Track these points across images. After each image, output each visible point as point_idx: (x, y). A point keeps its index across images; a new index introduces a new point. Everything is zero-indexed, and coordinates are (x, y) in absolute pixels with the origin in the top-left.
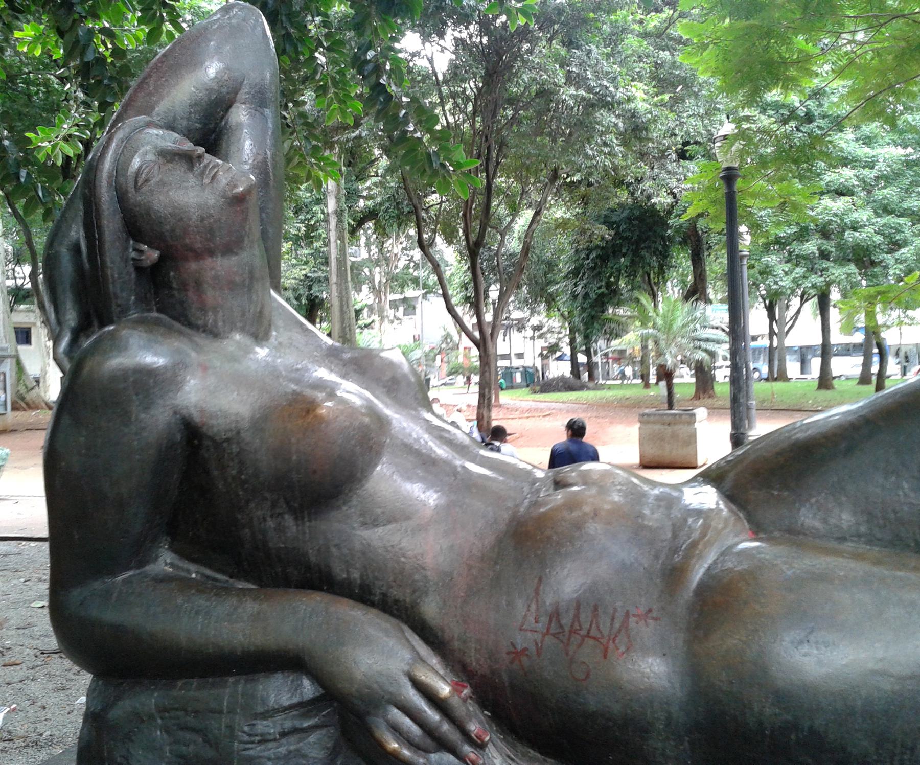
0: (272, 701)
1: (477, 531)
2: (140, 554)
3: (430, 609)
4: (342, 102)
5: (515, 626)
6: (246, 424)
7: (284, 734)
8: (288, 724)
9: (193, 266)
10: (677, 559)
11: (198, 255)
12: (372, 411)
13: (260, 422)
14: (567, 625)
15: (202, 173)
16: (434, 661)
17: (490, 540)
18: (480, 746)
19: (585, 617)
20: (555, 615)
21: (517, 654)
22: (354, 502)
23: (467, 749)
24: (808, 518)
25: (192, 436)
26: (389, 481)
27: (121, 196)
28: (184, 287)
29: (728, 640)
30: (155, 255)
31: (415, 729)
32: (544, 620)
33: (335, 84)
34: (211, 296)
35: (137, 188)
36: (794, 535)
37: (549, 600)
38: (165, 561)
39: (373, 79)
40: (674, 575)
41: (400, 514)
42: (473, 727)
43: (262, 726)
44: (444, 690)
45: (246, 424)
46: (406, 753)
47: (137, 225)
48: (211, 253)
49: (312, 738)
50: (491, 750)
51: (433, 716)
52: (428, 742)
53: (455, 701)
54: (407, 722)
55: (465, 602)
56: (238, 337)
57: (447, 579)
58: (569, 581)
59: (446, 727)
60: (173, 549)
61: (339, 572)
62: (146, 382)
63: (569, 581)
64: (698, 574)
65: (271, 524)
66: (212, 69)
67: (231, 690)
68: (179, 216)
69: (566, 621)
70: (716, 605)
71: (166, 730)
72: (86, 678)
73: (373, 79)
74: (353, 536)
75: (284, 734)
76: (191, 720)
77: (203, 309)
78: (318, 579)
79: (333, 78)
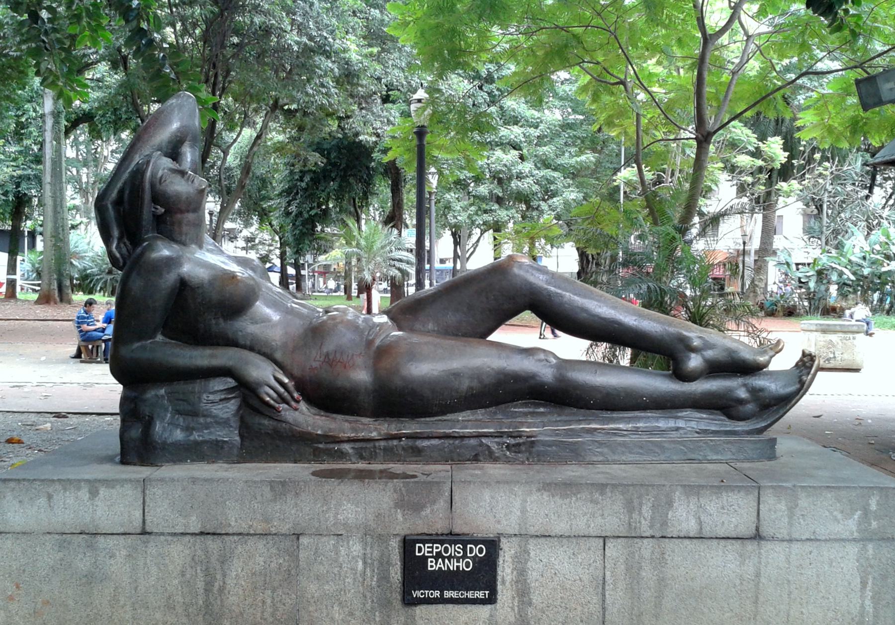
0: (216, 388)
1: (297, 327)
2: (153, 336)
3: (278, 356)
4: (94, 30)
5: (311, 362)
6: (206, 282)
7: (221, 400)
8: (223, 397)
9: (179, 216)
10: (371, 338)
11: (182, 212)
12: (253, 279)
13: (211, 282)
14: (330, 361)
15: (188, 179)
17: (301, 331)
19: (338, 355)
20: (327, 355)
21: (312, 369)
22: (248, 314)
23: (293, 403)
24: (418, 326)
25: (183, 285)
26: (262, 308)
27: (153, 186)
28: (173, 224)
29: (386, 363)
30: (163, 210)
31: (275, 395)
32: (323, 357)
33: (90, 15)
34: (185, 229)
35: (160, 183)
36: (412, 330)
37: (325, 351)
38: (160, 338)
39: (134, 23)
40: (370, 343)
41: (266, 320)
42: (296, 395)
43: (211, 397)
44: (286, 380)
45: (206, 282)
46: (272, 402)
47: (158, 197)
48: (188, 211)
49: (233, 401)
51: (282, 390)
52: (279, 400)
54: (271, 392)
55: (293, 352)
56: (194, 246)
57: (285, 345)
58: (330, 346)
59: (286, 394)
60: (163, 334)
61: (242, 342)
62: (171, 263)
63: (330, 346)
64: (377, 342)
65: (214, 322)
66: (175, 125)
67: (197, 386)
68: (178, 195)
69: (331, 357)
70: (381, 353)
72: (120, 387)
73: (134, 23)
74: (246, 327)
76: (181, 397)
77: (181, 234)
78: (232, 342)
79: (87, 10)
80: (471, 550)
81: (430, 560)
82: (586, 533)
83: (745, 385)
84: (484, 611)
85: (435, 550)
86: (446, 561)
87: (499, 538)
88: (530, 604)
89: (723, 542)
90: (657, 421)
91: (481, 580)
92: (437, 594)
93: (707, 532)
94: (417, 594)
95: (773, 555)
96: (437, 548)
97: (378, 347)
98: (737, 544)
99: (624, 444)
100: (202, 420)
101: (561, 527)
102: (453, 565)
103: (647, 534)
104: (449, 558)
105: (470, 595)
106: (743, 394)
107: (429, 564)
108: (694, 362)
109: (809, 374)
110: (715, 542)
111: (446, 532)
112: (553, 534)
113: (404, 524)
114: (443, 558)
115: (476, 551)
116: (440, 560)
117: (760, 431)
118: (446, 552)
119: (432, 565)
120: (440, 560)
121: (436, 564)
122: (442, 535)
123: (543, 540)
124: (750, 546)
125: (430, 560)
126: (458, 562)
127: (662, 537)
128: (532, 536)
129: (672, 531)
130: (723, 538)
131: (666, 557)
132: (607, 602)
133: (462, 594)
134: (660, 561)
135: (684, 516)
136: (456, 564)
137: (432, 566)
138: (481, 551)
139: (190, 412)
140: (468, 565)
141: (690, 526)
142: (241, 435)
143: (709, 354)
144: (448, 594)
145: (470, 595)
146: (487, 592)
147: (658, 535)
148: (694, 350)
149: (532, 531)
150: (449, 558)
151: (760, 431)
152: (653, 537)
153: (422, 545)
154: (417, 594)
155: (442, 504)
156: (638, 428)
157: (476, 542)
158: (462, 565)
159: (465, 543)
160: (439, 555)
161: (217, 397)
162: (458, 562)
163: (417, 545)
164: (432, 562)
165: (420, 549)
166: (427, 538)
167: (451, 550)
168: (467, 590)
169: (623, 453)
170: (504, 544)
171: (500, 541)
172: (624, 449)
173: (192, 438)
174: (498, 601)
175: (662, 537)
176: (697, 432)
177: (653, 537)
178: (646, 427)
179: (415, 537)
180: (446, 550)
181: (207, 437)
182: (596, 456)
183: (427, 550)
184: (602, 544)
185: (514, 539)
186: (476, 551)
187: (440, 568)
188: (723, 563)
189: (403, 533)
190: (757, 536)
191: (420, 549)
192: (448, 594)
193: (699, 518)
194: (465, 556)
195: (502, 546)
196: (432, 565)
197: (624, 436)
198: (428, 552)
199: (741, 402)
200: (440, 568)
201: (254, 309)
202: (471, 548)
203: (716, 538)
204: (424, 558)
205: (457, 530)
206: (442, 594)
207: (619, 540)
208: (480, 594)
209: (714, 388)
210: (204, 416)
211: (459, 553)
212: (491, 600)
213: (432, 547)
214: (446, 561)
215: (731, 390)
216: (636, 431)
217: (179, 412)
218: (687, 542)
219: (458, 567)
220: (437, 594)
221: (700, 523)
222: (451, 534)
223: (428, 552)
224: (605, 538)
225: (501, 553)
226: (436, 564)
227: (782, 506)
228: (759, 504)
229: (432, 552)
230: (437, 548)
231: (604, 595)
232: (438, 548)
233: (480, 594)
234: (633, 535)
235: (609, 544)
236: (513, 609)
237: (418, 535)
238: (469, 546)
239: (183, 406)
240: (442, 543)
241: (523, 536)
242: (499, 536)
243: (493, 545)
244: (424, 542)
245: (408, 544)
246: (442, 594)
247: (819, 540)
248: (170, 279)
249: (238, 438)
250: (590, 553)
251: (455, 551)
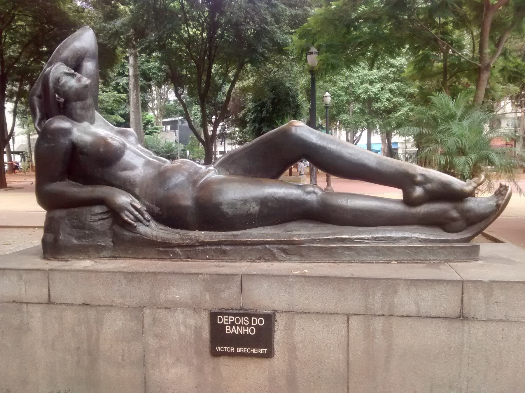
7: (100, 220)
16: (137, 201)
18: (148, 221)
43: (93, 218)
49: (106, 221)
50: (151, 222)
52: (135, 220)
53: (142, 209)
67: (85, 210)
71: (69, 220)
75: (100, 220)
76: (75, 218)
80: (255, 321)
81: (227, 327)
82: (335, 312)
83: (455, 208)
84: (265, 363)
85: (230, 320)
86: (238, 328)
87: (274, 313)
88: (296, 358)
89: (435, 320)
90: (391, 233)
91: (261, 340)
92: (232, 349)
93: (423, 312)
94: (219, 349)
95: (476, 331)
96: (232, 319)
97: (202, 183)
98: (446, 322)
99: (365, 249)
100: (87, 232)
101: (317, 306)
102: (243, 331)
103: (379, 313)
104: (240, 326)
105: (254, 351)
106: (455, 214)
107: (227, 329)
108: (418, 191)
109: (503, 200)
110: (430, 320)
111: (239, 308)
112: (311, 311)
113: (209, 301)
114: (236, 326)
115: (258, 321)
116: (234, 327)
117: (468, 240)
118: (238, 322)
119: (228, 330)
120: (234, 327)
121: (231, 329)
122: (236, 310)
123: (304, 315)
124: (457, 324)
125: (227, 327)
126: (246, 328)
127: (390, 315)
128: (297, 312)
129: (398, 311)
130: (436, 317)
131: (393, 329)
132: (351, 359)
133: (249, 350)
134: (388, 334)
135: (406, 301)
136: (244, 330)
137: (228, 331)
138: (261, 322)
139: (81, 228)
140: (252, 331)
141: (411, 308)
142: (113, 242)
143: (429, 186)
144: (239, 350)
145: (254, 351)
146: (266, 350)
147: (386, 314)
148: (419, 184)
149: (297, 308)
150: (240, 326)
151: (468, 240)
152: (383, 315)
153: (221, 317)
154: (219, 349)
155: (235, 288)
156: (376, 238)
157: (258, 316)
158: (248, 331)
159: (250, 316)
160: (233, 324)
161: (96, 218)
162: (246, 328)
163: (218, 317)
164: (228, 328)
165: (220, 318)
166: (224, 311)
167: (241, 320)
168: (253, 347)
169: (365, 255)
170: (278, 317)
171: (275, 316)
172: (366, 253)
173: (81, 243)
174: (275, 356)
175: (390, 315)
176: (420, 241)
177: (383, 315)
178: (382, 237)
179: (217, 311)
180: (238, 320)
181: (91, 243)
182: (346, 257)
183: (225, 320)
184: (346, 319)
185: (284, 314)
186: (258, 321)
187: (234, 332)
188: (436, 335)
189: (210, 308)
190: (462, 317)
191: (220, 319)
192: (239, 350)
193: (418, 303)
194: (250, 325)
195: (277, 318)
196: (228, 330)
197: (366, 243)
198: (226, 321)
199: (454, 220)
200: (234, 332)
201: (122, 161)
202: (254, 320)
203: (430, 317)
204: (223, 326)
205: (246, 307)
206: (235, 350)
207: (360, 318)
208: (260, 351)
209: (434, 210)
210: (89, 229)
211: (246, 323)
212: (269, 355)
213: (228, 318)
214: (238, 328)
215: (445, 212)
216: (375, 239)
217: (74, 227)
218: (408, 320)
219: (246, 332)
220: (232, 349)
221: (418, 307)
222: (242, 309)
223: (226, 321)
224: (348, 316)
225: (276, 323)
226: (231, 329)
227: (481, 295)
228: (463, 293)
229: (228, 322)
230: (232, 319)
231: (348, 355)
232: (232, 319)
233: (260, 351)
234: (369, 314)
235: (353, 319)
236: (284, 361)
237: (219, 309)
238: (253, 318)
239: (76, 222)
240: (235, 315)
241: (291, 313)
242: (275, 311)
243: (270, 318)
244: (223, 314)
245: (213, 316)
246: (235, 350)
247: (510, 321)
248: (64, 141)
249: (112, 244)
250: (338, 326)
251: (244, 321)
